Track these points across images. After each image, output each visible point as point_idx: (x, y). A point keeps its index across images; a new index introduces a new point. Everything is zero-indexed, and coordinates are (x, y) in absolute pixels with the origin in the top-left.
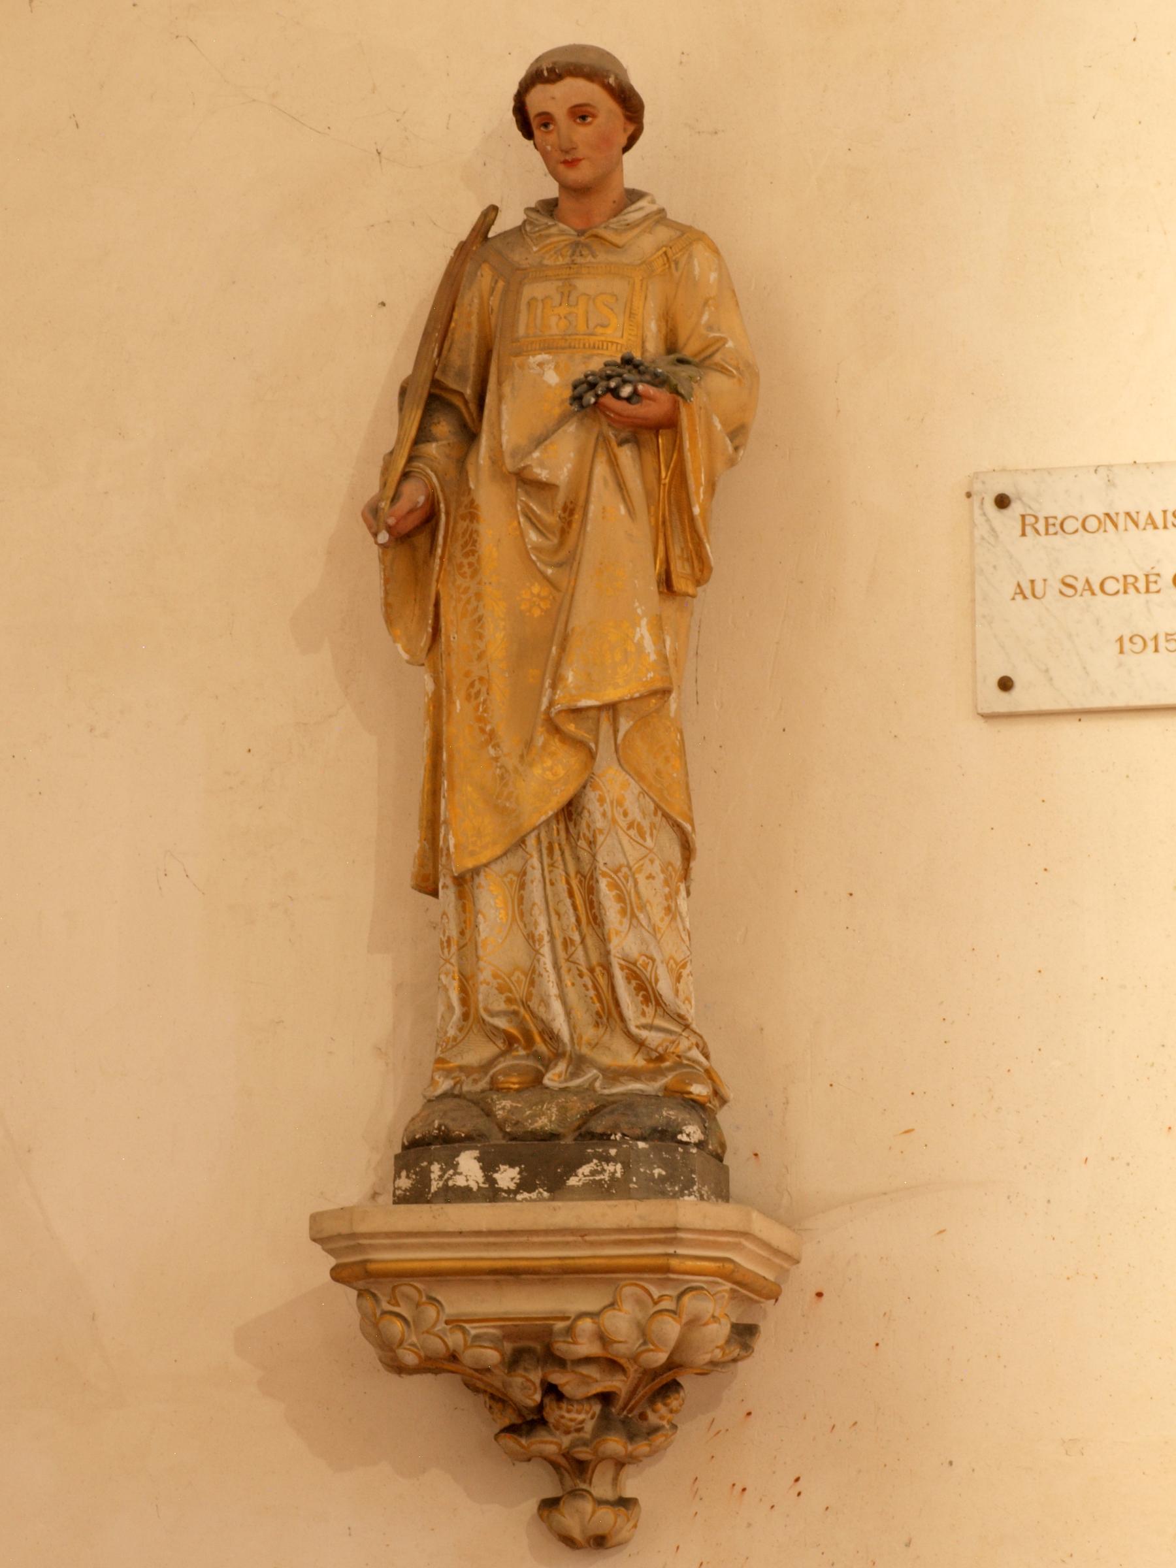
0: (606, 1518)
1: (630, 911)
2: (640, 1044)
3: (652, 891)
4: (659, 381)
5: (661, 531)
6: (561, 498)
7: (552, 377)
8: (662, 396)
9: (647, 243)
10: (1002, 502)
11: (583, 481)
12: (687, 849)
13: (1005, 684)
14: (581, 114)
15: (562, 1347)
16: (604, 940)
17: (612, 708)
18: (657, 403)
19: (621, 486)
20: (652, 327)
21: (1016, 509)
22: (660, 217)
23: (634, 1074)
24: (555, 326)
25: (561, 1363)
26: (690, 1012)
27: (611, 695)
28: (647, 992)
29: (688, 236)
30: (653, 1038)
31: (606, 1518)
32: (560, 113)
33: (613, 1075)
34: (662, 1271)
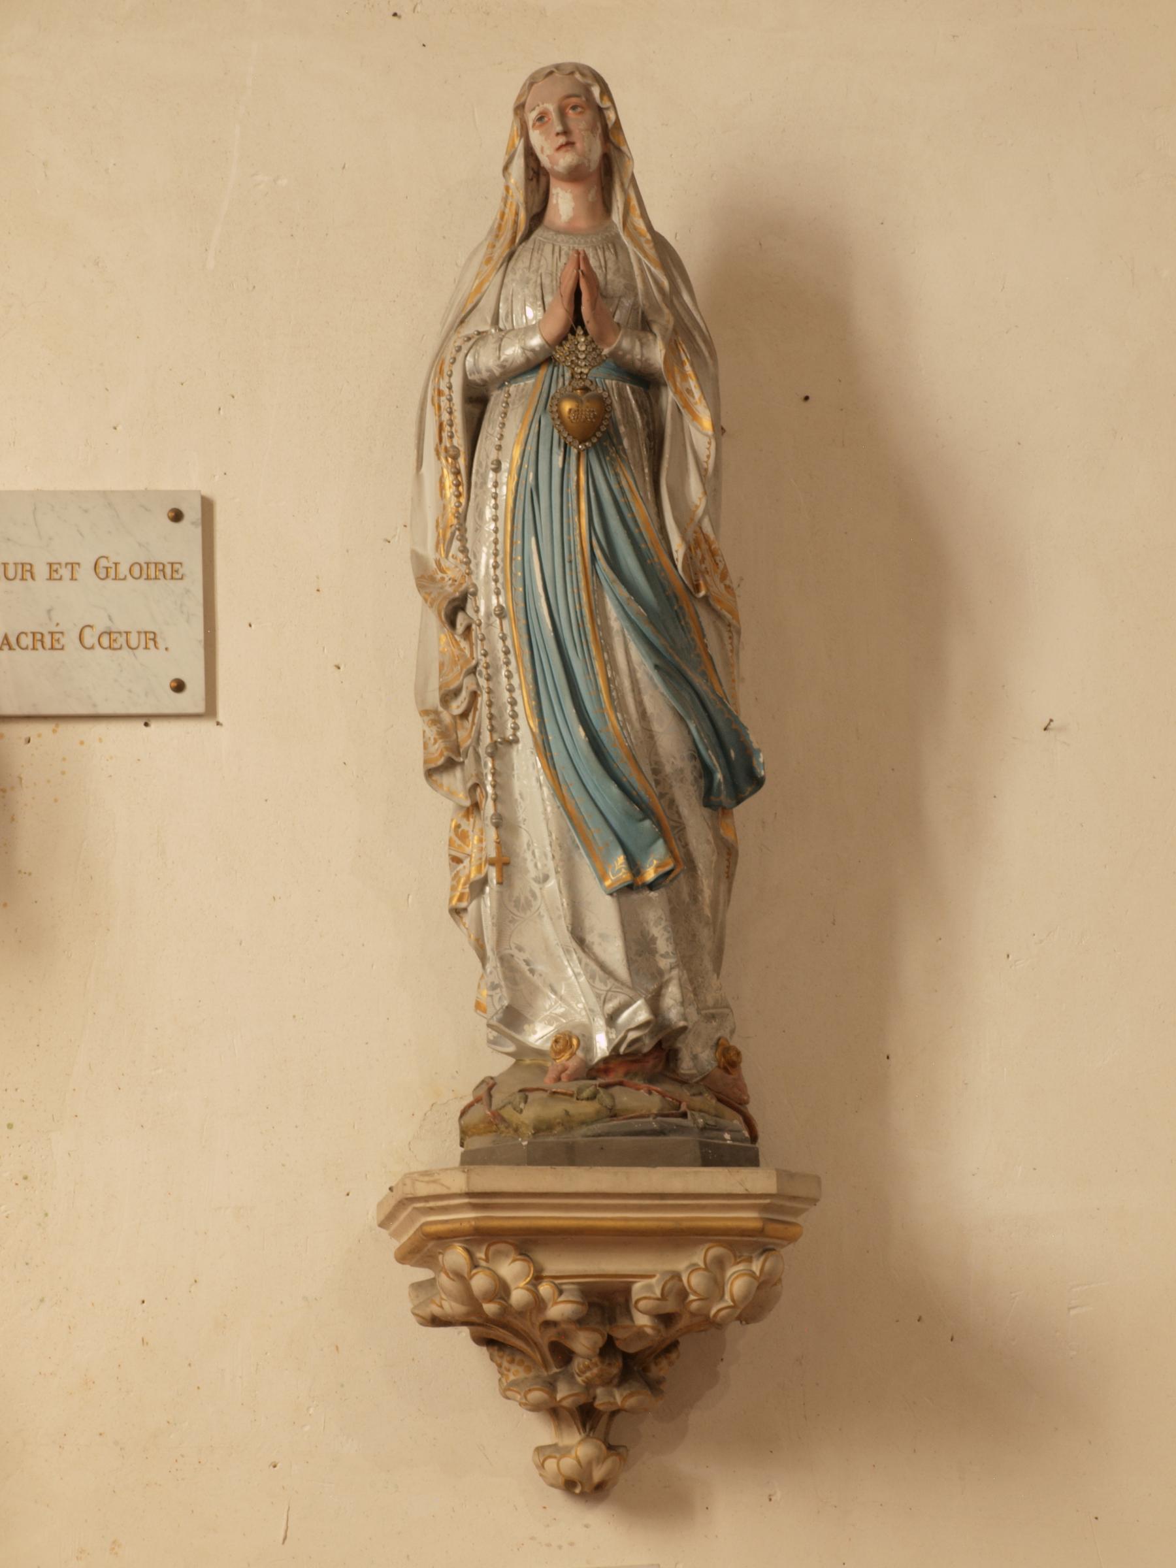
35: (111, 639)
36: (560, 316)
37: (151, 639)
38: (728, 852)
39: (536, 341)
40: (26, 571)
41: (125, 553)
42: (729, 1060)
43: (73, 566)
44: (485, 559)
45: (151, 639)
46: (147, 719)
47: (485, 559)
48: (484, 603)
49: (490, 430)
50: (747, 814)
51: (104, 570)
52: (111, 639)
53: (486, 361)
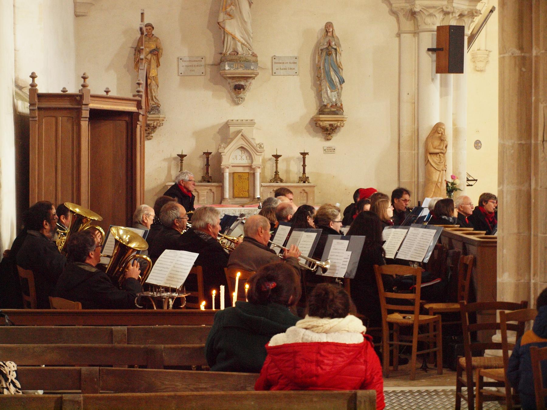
0: (151, 138)
1: (154, 92)
2: (155, 102)
3: (156, 90)
4: (157, 51)
5: (157, 62)
6: (149, 60)
7: (148, 50)
8: (157, 52)
9: (154, 39)
10: (181, 59)
11: (151, 59)
12: (158, 87)
13: (181, 73)
14: (150, 29)
15: (150, 125)
16: (152, 94)
17: (153, 77)
18: (157, 52)
19: (154, 59)
20: (155, 46)
21: (182, 60)
22: (155, 37)
23: (154, 104)
24: (148, 46)
25: (150, 126)
26: (158, 99)
27: (153, 75)
28: (155, 98)
29: (157, 38)
30: (156, 101)
31: (151, 138)
32: (148, 29)
33: (153, 104)
34: (158, 120)
35: (291, 69)
36: (328, 44)
37: (294, 69)
38: (342, 88)
39: (326, 46)
40: (284, 63)
41: (292, 61)
42: (342, 105)
43: (288, 63)
44: (322, 64)
45: (294, 69)
46: (294, 75)
47: (322, 64)
48: (322, 68)
49: (322, 53)
50: (343, 85)
51: (290, 63)
52: (291, 69)
53: (322, 48)
